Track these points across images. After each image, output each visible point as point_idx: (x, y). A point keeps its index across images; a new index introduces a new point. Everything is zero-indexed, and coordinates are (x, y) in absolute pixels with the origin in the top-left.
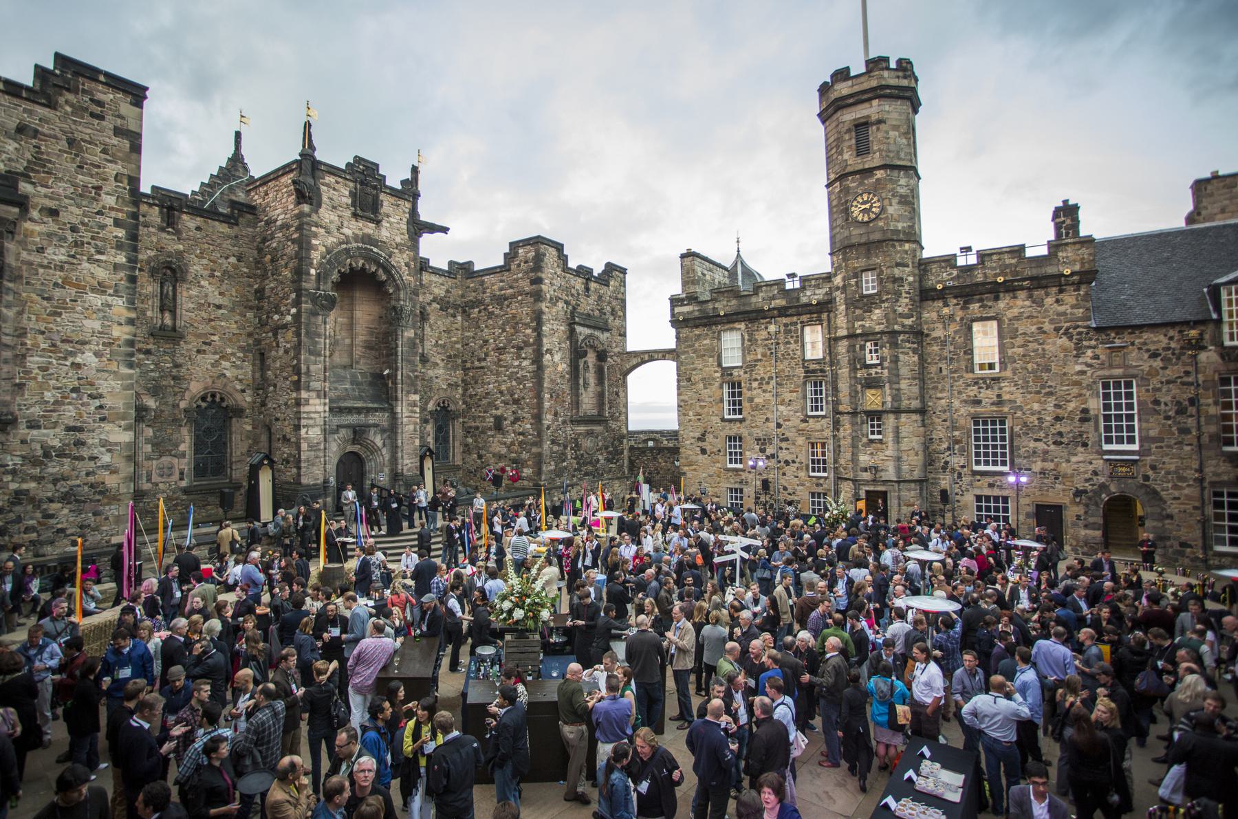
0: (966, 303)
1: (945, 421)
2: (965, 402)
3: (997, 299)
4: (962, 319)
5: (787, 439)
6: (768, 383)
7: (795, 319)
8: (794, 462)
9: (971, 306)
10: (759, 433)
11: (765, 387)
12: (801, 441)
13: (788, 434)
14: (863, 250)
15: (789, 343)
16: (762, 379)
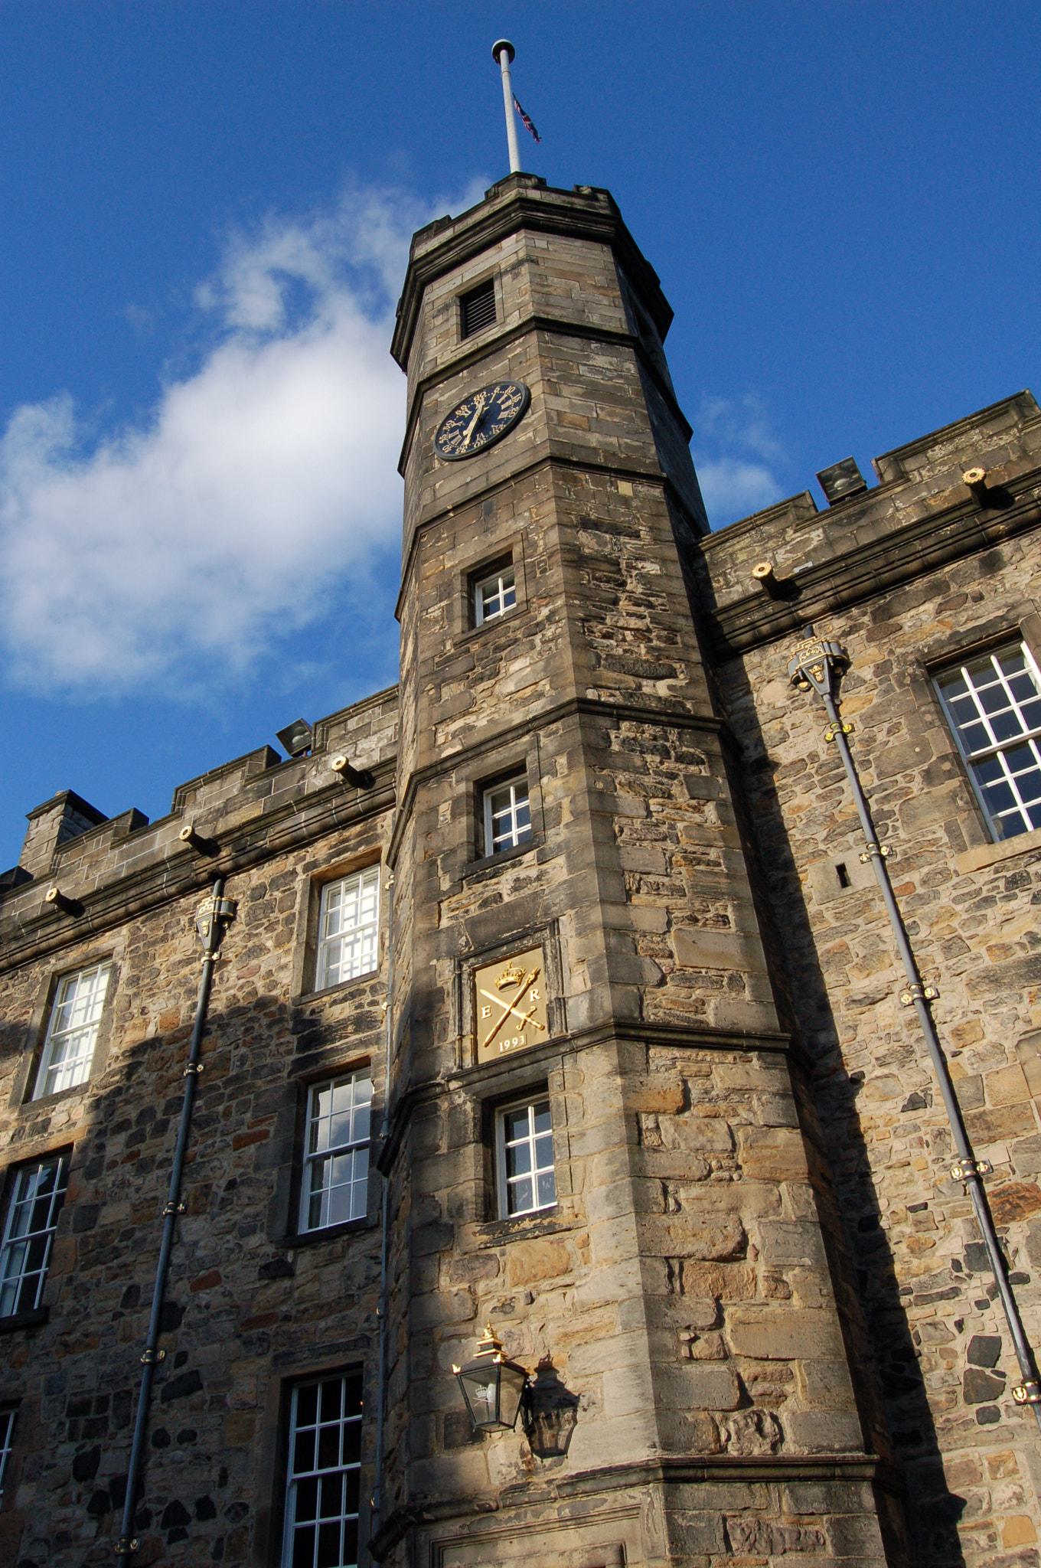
0: (883, 615)
1: (915, 1103)
2: (994, 979)
3: (992, 565)
4: (882, 669)
5: (190, 1384)
6: (162, 1128)
7: (288, 862)
8: (206, 1509)
9: (906, 620)
10: (85, 1372)
11: (145, 1149)
12: (251, 1381)
13: (203, 1355)
14: (471, 516)
15: (260, 950)
16: (146, 1114)
